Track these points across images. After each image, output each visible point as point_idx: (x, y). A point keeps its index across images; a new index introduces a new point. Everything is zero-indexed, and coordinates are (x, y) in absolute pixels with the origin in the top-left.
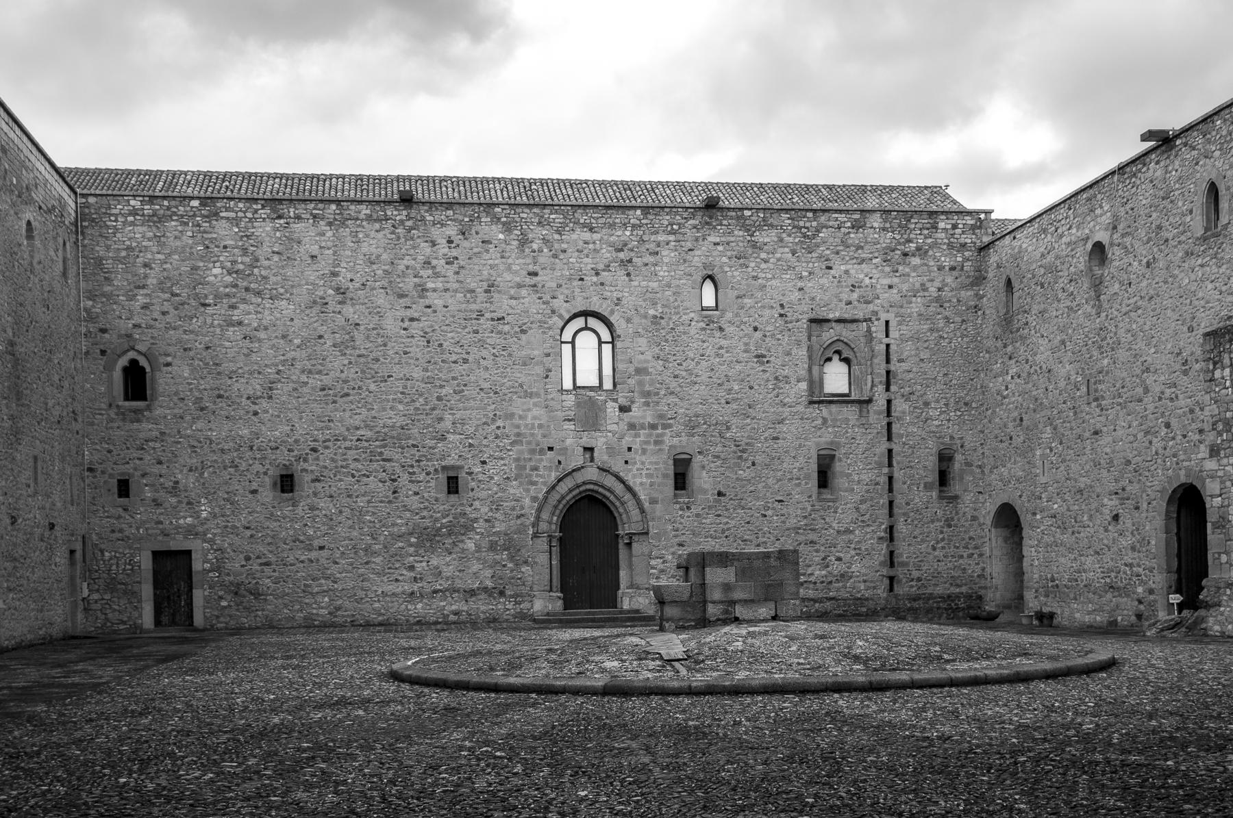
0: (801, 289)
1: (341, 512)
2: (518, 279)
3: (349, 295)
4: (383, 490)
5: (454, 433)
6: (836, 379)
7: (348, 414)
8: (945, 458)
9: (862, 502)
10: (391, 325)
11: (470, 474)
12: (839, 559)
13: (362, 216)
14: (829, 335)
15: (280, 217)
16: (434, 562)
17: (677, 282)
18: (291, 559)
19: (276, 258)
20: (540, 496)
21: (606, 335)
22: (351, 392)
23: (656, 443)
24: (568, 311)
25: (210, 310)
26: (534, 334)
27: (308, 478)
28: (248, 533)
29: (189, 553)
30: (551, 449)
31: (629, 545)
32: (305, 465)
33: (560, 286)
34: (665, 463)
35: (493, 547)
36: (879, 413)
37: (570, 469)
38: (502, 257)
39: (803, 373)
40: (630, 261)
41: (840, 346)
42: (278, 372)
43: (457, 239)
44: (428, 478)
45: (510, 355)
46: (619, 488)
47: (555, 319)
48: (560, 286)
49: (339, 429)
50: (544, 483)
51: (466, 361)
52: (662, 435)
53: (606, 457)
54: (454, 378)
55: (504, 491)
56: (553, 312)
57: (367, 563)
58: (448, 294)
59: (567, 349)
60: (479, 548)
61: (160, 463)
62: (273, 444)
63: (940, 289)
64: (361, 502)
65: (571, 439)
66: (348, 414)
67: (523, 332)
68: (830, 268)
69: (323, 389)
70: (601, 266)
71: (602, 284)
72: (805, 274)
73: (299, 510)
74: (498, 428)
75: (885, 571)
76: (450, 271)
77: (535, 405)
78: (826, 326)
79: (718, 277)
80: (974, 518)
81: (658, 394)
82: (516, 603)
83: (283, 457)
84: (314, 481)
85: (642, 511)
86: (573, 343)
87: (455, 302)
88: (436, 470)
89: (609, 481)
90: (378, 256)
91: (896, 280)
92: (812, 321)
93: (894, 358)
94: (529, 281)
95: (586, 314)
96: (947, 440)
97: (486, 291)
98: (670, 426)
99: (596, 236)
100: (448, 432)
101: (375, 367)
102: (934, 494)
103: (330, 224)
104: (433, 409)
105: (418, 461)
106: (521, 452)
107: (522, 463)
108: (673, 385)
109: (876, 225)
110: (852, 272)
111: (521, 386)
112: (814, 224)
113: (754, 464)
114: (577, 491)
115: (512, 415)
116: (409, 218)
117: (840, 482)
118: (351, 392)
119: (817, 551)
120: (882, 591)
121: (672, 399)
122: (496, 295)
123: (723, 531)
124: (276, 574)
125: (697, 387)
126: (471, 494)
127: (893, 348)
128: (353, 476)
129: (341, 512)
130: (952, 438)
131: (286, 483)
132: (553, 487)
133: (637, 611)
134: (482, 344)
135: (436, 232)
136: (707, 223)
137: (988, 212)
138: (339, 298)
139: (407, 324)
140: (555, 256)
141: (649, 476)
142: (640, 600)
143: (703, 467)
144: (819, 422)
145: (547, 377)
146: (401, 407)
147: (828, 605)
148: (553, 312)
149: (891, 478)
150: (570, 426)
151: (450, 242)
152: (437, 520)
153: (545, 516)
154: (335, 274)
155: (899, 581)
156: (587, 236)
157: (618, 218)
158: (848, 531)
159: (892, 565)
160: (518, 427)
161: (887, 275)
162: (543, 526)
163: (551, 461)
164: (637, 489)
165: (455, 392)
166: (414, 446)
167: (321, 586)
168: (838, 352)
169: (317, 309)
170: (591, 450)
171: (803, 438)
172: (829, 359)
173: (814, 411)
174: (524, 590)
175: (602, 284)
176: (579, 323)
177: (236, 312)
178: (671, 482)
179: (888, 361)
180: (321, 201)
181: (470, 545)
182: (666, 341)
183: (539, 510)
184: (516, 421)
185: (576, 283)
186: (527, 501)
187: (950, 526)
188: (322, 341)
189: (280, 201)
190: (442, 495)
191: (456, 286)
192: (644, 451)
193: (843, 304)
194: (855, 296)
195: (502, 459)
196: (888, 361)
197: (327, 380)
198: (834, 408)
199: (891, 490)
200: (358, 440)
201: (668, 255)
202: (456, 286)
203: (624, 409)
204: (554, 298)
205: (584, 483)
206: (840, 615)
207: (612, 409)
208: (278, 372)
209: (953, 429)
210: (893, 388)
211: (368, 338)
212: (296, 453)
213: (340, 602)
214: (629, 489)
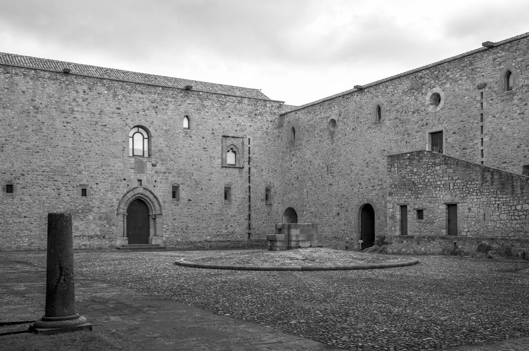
0: (220, 124)
1: (34, 202)
2: (112, 110)
3: (40, 110)
4: (54, 194)
5: (85, 171)
6: (231, 159)
7: (38, 160)
8: (268, 190)
9: (240, 205)
10: (58, 124)
11: (91, 188)
12: (231, 226)
13: (46, 77)
14: (229, 142)
15: (8, 73)
17: (175, 117)
18: (11, 222)
19: (6, 90)
20: (120, 198)
21: (146, 136)
22: (40, 151)
23: (166, 179)
24: (132, 125)
26: (119, 133)
27: (19, 187)
30: (125, 180)
31: (154, 219)
32: (18, 181)
33: (129, 114)
34: (169, 187)
35: (100, 219)
36: (246, 172)
38: (106, 100)
39: (220, 156)
40: (157, 107)
41: (232, 147)
43: (88, 91)
44: (73, 189)
45: (109, 140)
46: (151, 197)
47: (127, 127)
48: (129, 114)
49: (35, 166)
50: (122, 193)
51: (90, 142)
52: (168, 176)
53: (146, 184)
54: (85, 148)
55: (105, 196)
56: (127, 125)
58: (83, 114)
59: (131, 139)
60: (94, 219)
62: (3, 171)
63: (267, 129)
64: (44, 198)
65: (133, 176)
66: (38, 160)
67: (114, 131)
68: (230, 117)
69: (27, 149)
70: (146, 108)
71: (146, 115)
72: (221, 118)
73: (15, 201)
74: (103, 170)
75: (247, 231)
76: (84, 104)
77: (119, 161)
78: (228, 138)
79: (190, 116)
80: (277, 212)
81: (166, 160)
82: (110, 241)
83: (8, 177)
84: (22, 188)
85: (160, 206)
86: (133, 137)
87: (86, 117)
88: (77, 186)
89: (148, 194)
90: (53, 95)
91: (253, 124)
92: (224, 136)
93: (251, 152)
94: (117, 111)
95: (138, 126)
96: (269, 183)
97: (99, 114)
98: (171, 173)
99: (144, 96)
101: (51, 141)
102: (264, 203)
103: (31, 79)
104: (76, 160)
105: (69, 182)
106: (113, 180)
107: (113, 185)
108: (172, 157)
109: (246, 103)
110: (238, 119)
111: (113, 153)
112: (225, 100)
113: (202, 189)
114: (134, 197)
115: (109, 165)
116: (67, 80)
117: (233, 197)
118: (40, 151)
119: (224, 223)
120: (246, 239)
121: (172, 163)
122: (103, 116)
123: (190, 215)
124: (4, 228)
125: (181, 158)
126: (92, 196)
127: (251, 148)
128: (40, 187)
129: (34, 202)
130: (270, 183)
131: (9, 188)
132: (125, 195)
133: (159, 245)
134: (97, 135)
135: (79, 87)
136: (186, 96)
137: (283, 102)
138: (35, 110)
139: (65, 124)
140: (128, 102)
141: (163, 192)
142: (159, 240)
143: (183, 190)
144: (225, 174)
145: (124, 150)
147: (228, 243)
148: (127, 125)
149: (250, 197)
151: (84, 92)
152: (77, 207)
153: (122, 206)
154: (33, 100)
155: (252, 235)
156: (140, 95)
157: (153, 90)
158: (235, 216)
159: (250, 229)
160: (112, 170)
161: (250, 122)
162: (121, 211)
163: (124, 184)
164: (158, 197)
166: (67, 175)
167: (24, 233)
168: (232, 149)
169: (24, 115)
171: (220, 180)
172: (228, 151)
173: (224, 170)
174: (113, 236)
175: (146, 115)
176: (136, 130)
178: (171, 195)
179: (249, 153)
180: (28, 68)
182: (170, 140)
184: (111, 168)
185: (136, 114)
186: (115, 200)
187: (269, 215)
188: (27, 128)
189: (8, 66)
190: (80, 197)
191: (86, 110)
192: (161, 182)
193: (234, 131)
194: (238, 128)
196: (249, 153)
197: (30, 145)
198: (231, 169)
199: (250, 201)
200: (43, 172)
201: (171, 106)
202: (86, 110)
203: (153, 165)
204: (127, 119)
205: (138, 194)
206: (232, 247)
207: (149, 165)
209: (271, 180)
210: (251, 163)
211: (48, 129)
212: (14, 176)
213: (33, 240)
214: (155, 197)
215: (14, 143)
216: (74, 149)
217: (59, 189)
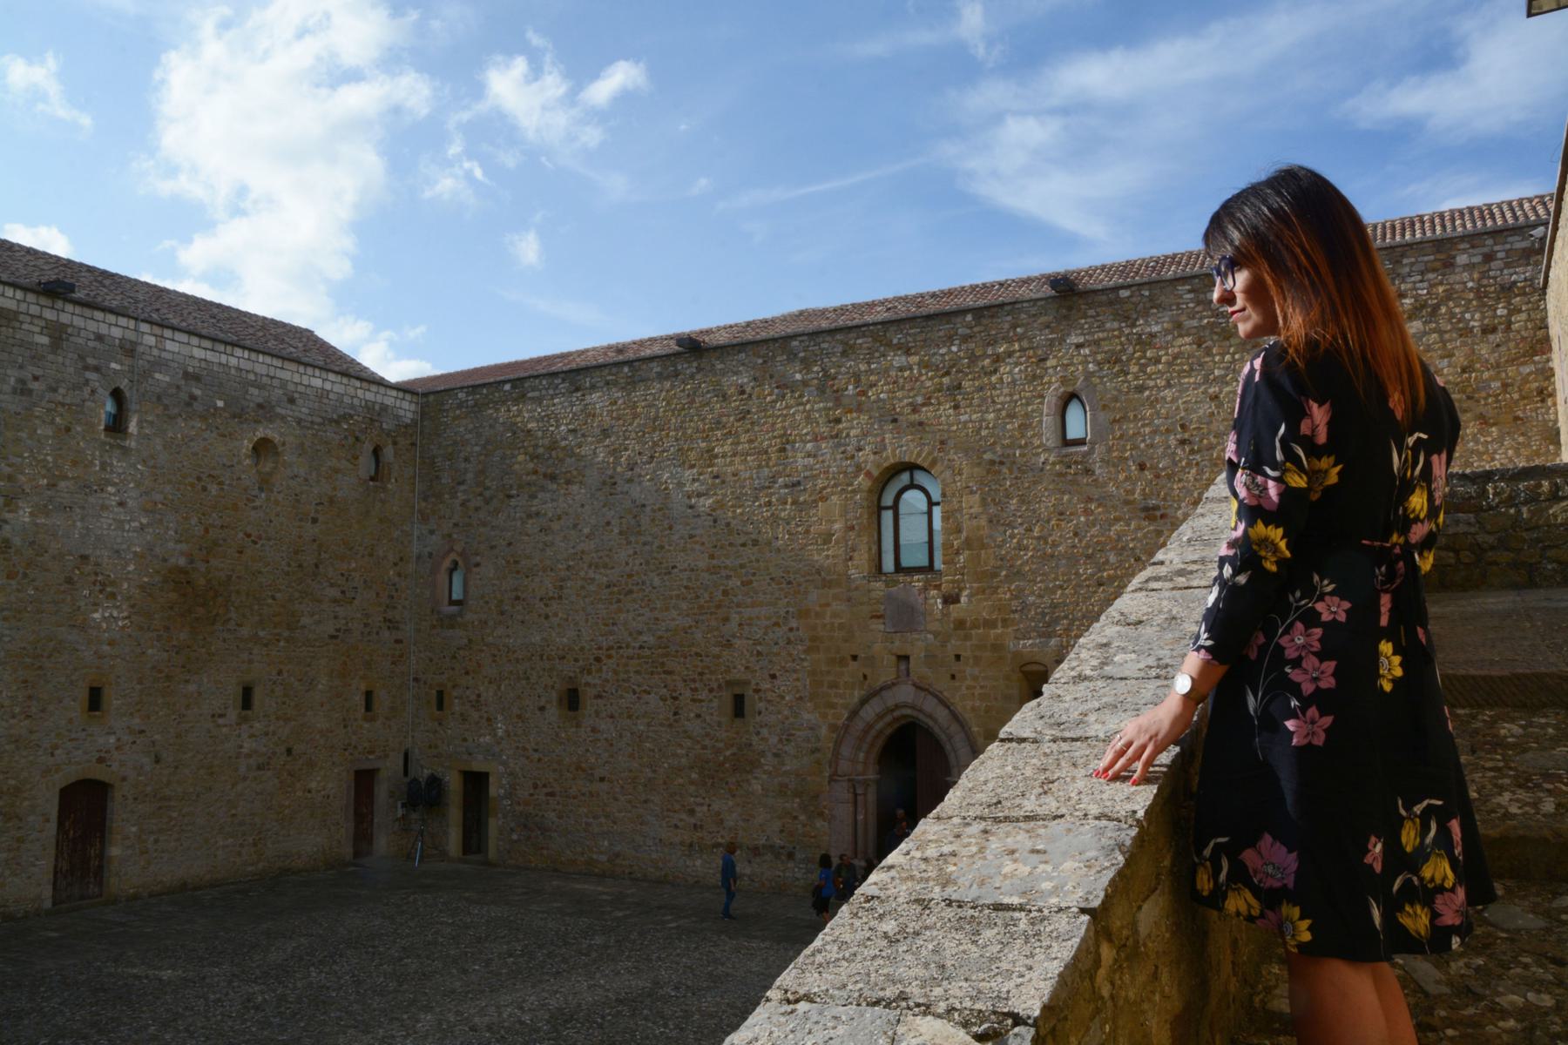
0: (1215, 398)
11: (757, 691)
16: (715, 807)
25: (513, 502)
27: (591, 692)
28: (536, 756)
29: (486, 775)
30: (855, 658)
32: (589, 679)
37: (878, 685)
42: (569, 568)
46: (942, 714)
54: (742, 566)
57: (646, 802)
59: (887, 516)
61: (467, 673)
69: (608, 586)
74: (791, 630)
88: (720, 686)
89: (930, 705)
99: (914, 359)
100: (734, 636)
104: (719, 607)
105: (701, 674)
114: (889, 718)
126: (758, 719)
131: (572, 700)
136: (1066, 317)
146: (684, 606)
150: (878, 626)
152: (718, 751)
153: (846, 751)
157: (943, 329)
162: (844, 766)
165: (743, 583)
166: (697, 654)
170: (906, 658)
177: (535, 502)
181: (757, 787)
183: (838, 743)
186: (824, 731)
192: (977, 660)
195: (795, 671)
205: (897, 707)
208: (569, 568)
212: (581, 663)
214: (955, 716)
215: (582, 574)
216: (713, 570)
217: (675, 699)
